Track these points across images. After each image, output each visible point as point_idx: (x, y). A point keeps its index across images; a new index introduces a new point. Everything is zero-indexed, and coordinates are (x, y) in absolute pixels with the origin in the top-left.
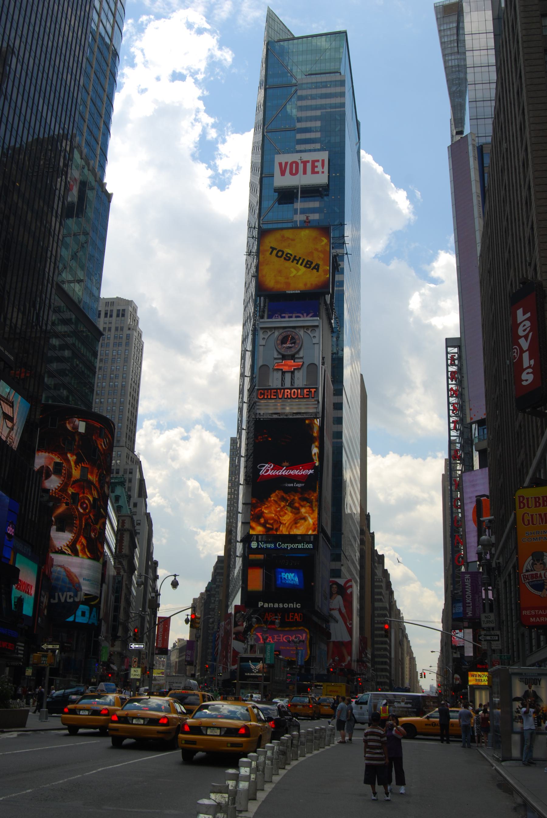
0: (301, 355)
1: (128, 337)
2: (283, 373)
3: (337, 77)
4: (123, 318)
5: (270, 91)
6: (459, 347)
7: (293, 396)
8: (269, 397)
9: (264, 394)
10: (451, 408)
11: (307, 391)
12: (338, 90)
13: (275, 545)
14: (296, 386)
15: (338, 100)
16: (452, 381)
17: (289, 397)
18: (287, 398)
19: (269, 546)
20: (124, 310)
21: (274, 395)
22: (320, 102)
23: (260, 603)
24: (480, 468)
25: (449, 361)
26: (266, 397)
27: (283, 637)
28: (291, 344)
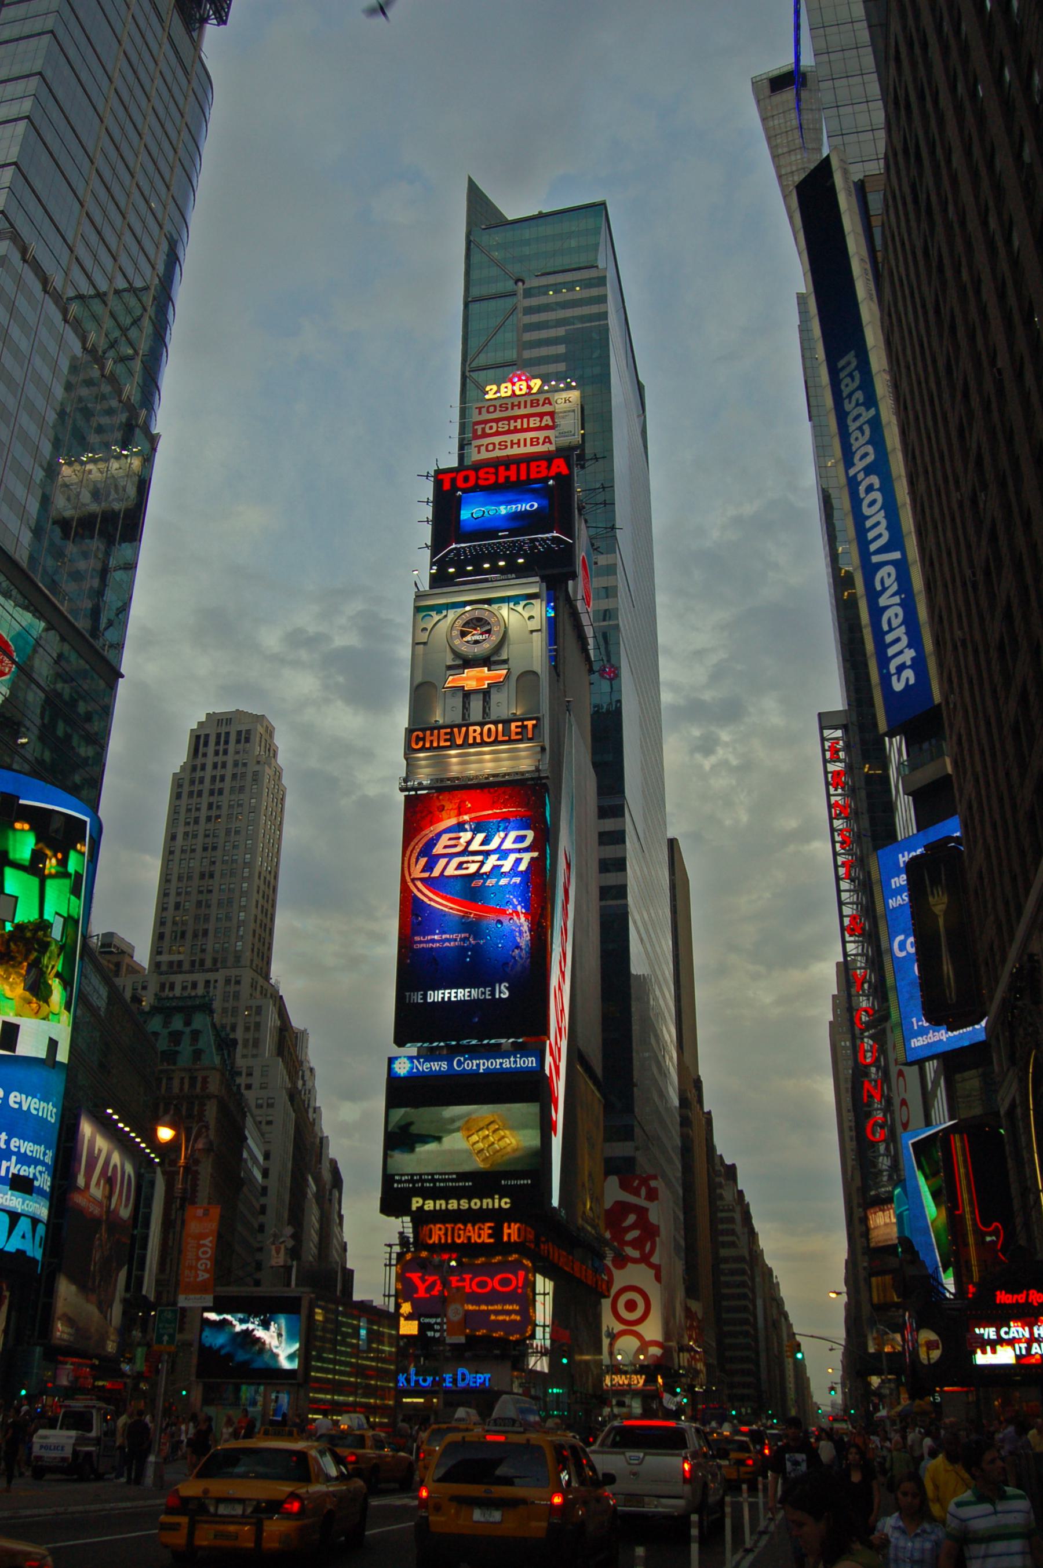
0: (505, 657)
1: (256, 777)
2: (467, 695)
3: (592, 273)
4: (248, 745)
5: (474, 307)
6: (845, 728)
7: (486, 739)
8: (435, 744)
9: (424, 739)
10: (838, 838)
11: (517, 727)
12: (595, 292)
13: (450, 1065)
14: (493, 717)
15: (595, 309)
16: (836, 790)
17: (478, 740)
18: (475, 744)
19: (435, 1066)
20: (248, 732)
21: (446, 740)
22: (561, 314)
23: (414, 1200)
24: (919, 828)
25: (828, 754)
26: (428, 745)
27: (471, 1280)
28: (482, 634)
